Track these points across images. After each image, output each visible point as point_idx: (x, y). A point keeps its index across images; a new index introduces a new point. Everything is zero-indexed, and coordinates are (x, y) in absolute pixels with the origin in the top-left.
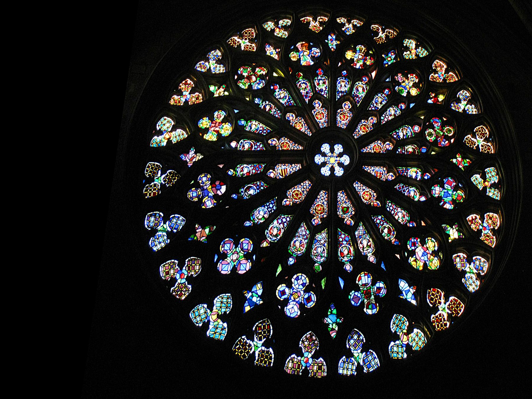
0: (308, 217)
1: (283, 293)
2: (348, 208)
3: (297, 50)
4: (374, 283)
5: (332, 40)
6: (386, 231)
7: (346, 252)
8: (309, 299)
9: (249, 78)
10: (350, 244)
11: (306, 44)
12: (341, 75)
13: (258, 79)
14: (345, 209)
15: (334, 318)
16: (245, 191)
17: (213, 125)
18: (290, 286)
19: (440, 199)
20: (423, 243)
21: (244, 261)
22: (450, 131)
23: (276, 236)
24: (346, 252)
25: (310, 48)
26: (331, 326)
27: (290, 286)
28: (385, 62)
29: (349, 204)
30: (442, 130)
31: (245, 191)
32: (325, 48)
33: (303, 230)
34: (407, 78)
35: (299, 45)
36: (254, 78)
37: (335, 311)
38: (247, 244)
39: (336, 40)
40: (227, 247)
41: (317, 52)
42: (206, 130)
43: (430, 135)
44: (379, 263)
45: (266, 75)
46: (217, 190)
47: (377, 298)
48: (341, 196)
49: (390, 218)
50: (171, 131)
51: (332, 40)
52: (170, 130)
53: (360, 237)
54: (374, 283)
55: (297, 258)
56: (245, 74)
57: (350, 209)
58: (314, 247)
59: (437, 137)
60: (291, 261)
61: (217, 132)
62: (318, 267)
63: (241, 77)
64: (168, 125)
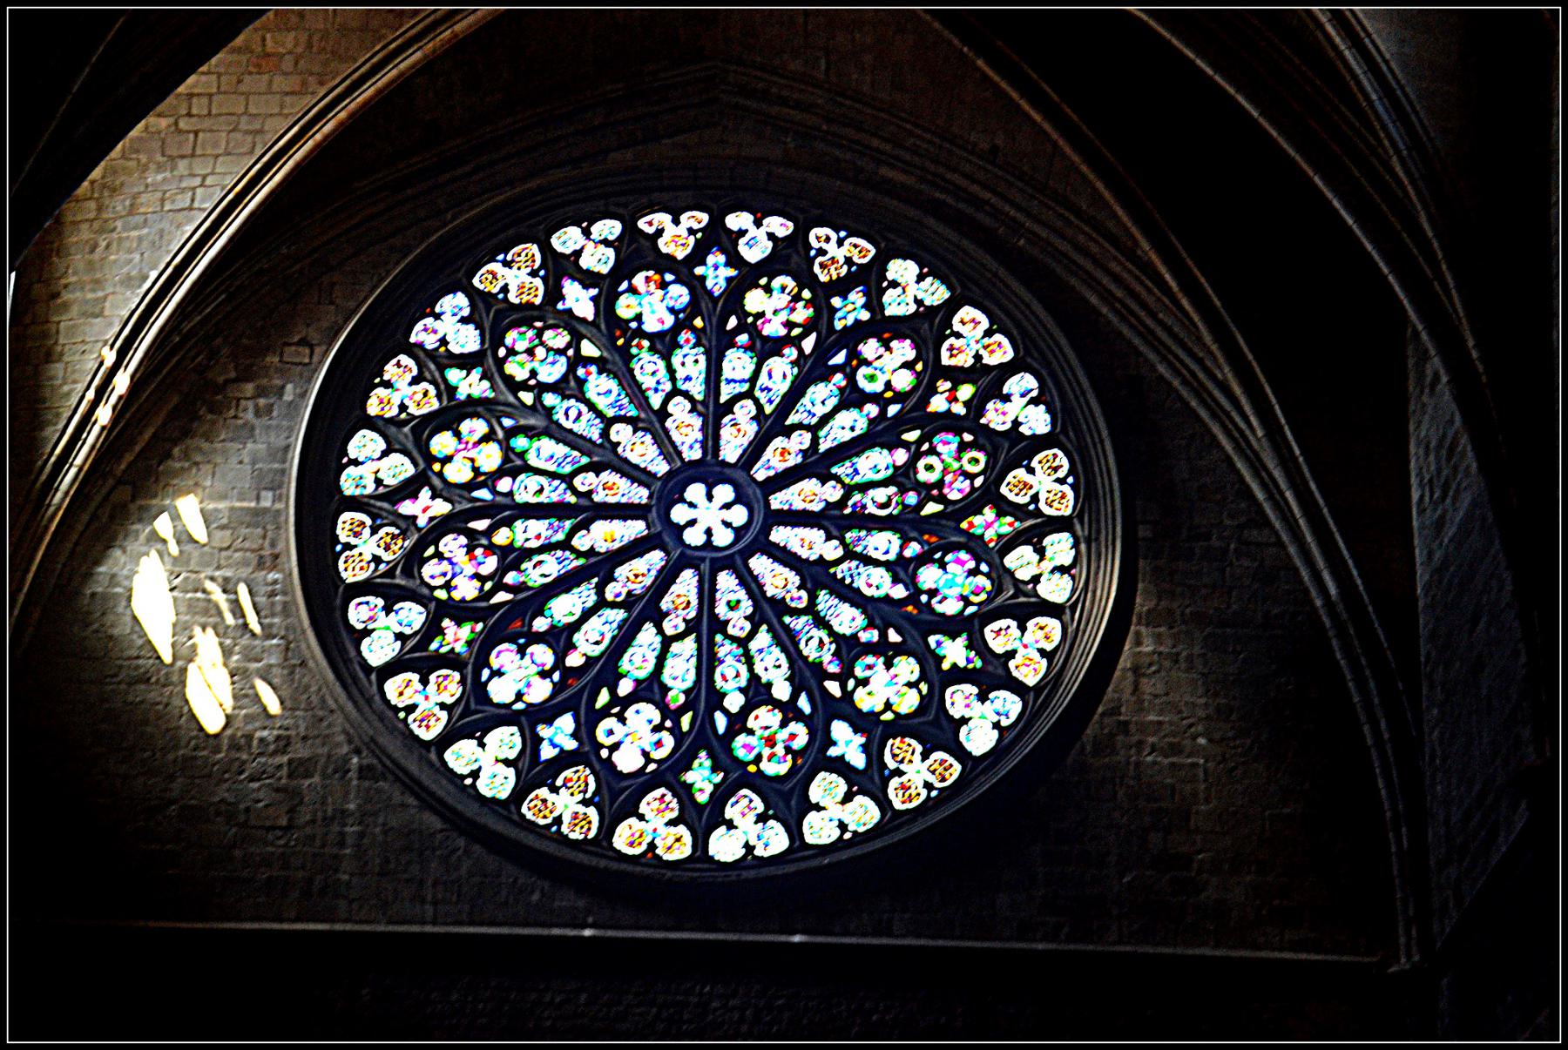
0: (658, 618)
1: (610, 732)
2: (738, 602)
3: (633, 290)
4: (784, 724)
5: (716, 267)
6: (814, 643)
7: (730, 674)
8: (659, 744)
9: (530, 352)
10: (739, 661)
11: (657, 277)
12: (733, 345)
13: (552, 353)
14: (733, 604)
15: (707, 772)
16: (535, 567)
17: (463, 446)
18: (622, 720)
19: (933, 593)
20: (889, 665)
21: (536, 680)
22: (977, 461)
23: (597, 643)
24: (730, 674)
25: (663, 285)
26: (697, 786)
27: (622, 720)
28: (839, 315)
29: (742, 594)
30: (958, 459)
31: (535, 567)
32: (696, 286)
33: (648, 637)
34: (889, 349)
35: (639, 280)
36: (540, 352)
37: (708, 763)
38: (543, 654)
39: (727, 264)
40: (504, 656)
41: (680, 294)
42: (448, 459)
43: (929, 468)
44: (795, 696)
45: (569, 346)
46: (480, 564)
47: (788, 750)
48: (726, 581)
49: (821, 622)
50: (379, 459)
51: (716, 267)
52: (378, 455)
53: (761, 651)
54: (784, 724)
55: (637, 682)
56: (521, 346)
57: (742, 605)
58: (669, 662)
59: (945, 471)
60: (625, 687)
61: (472, 460)
62: (676, 698)
63: (512, 352)
64: (371, 446)
